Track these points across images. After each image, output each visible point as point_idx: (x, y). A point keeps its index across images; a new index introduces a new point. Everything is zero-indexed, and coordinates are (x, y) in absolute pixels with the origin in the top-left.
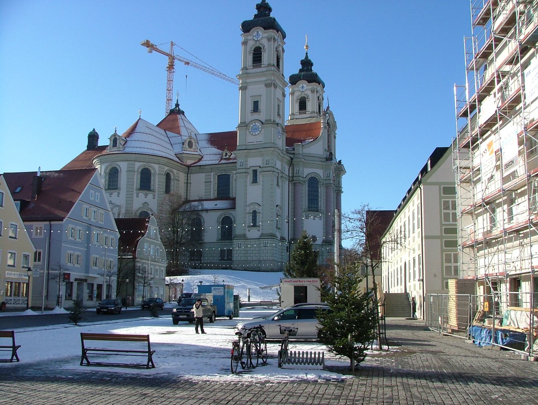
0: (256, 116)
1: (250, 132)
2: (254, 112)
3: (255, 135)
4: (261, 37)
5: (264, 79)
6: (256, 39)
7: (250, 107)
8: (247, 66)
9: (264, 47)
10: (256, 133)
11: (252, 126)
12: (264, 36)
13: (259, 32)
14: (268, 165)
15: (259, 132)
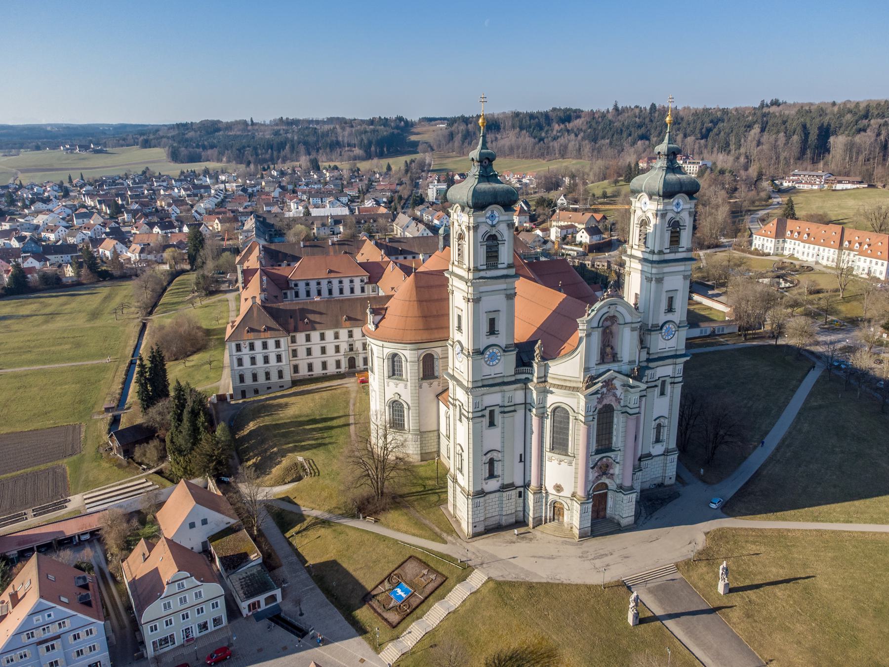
0: (493, 340)
1: (486, 362)
2: (490, 334)
3: (493, 365)
4: (497, 219)
5: (504, 286)
6: (490, 223)
7: (485, 327)
8: (479, 265)
9: (502, 235)
10: (494, 363)
11: (488, 353)
12: (502, 218)
13: (495, 212)
14: (510, 404)
15: (497, 361)
